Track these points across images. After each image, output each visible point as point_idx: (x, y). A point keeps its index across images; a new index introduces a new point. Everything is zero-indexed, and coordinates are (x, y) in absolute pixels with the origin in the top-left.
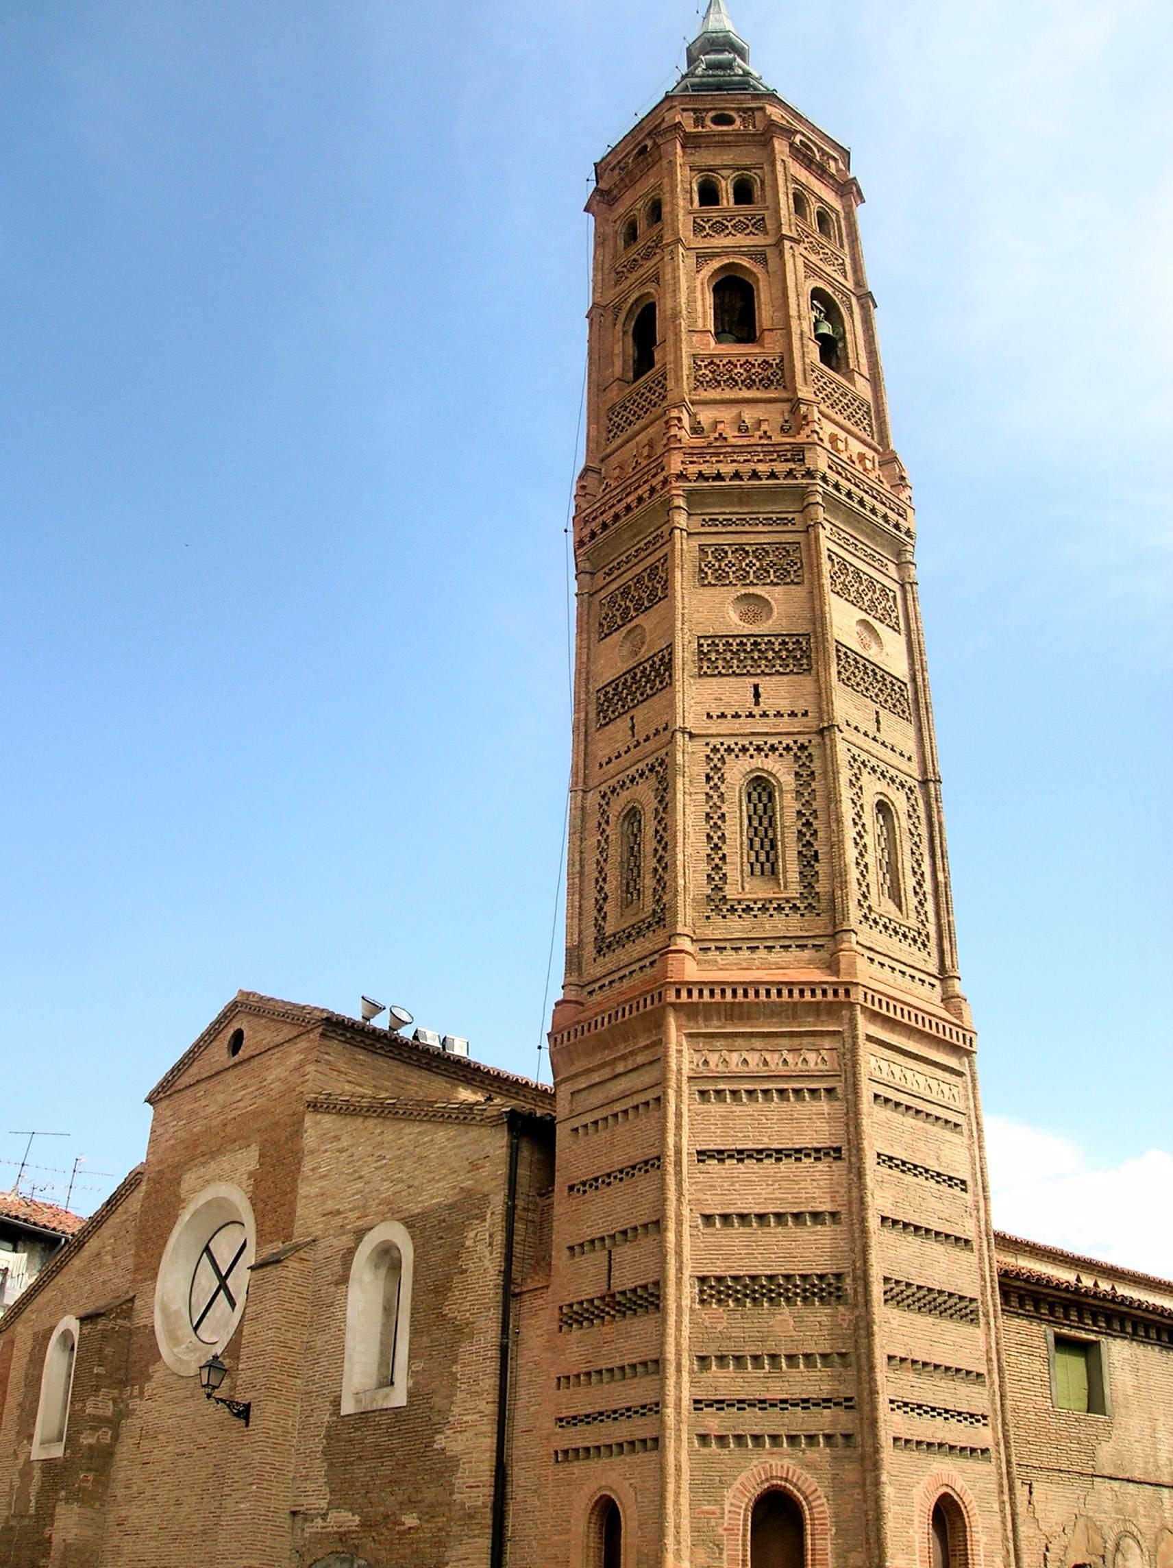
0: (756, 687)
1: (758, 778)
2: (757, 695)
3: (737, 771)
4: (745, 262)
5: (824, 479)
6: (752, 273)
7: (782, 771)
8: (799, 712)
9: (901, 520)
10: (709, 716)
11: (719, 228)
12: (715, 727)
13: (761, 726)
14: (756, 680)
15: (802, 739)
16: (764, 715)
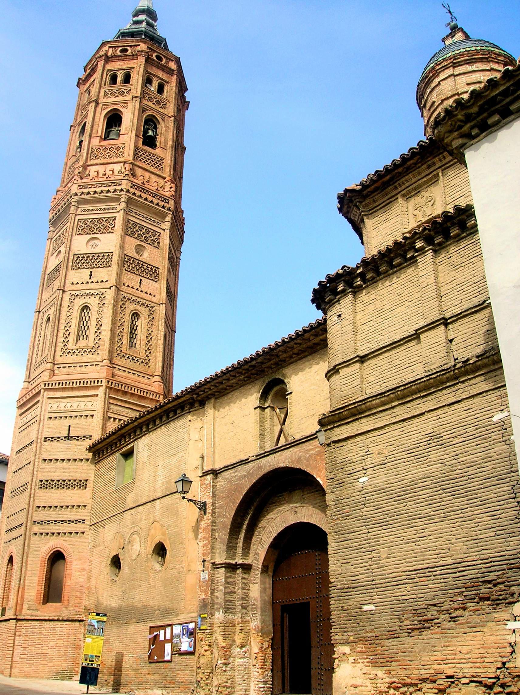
0: (91, 272)
1: (86, 306)
2: (91, 275)
3: (79, 302)
4: (118, 107)
5: (128, 191)
6: (121, 112)
7: (93, 302)
8: (104, 280)
9: (166, 204)
10: (73, 284)
11: (113, 94)
12: (74, 287)
13: (90, 286)
14: (91, 270)
15: (103, 291)
16: (92, 282)
